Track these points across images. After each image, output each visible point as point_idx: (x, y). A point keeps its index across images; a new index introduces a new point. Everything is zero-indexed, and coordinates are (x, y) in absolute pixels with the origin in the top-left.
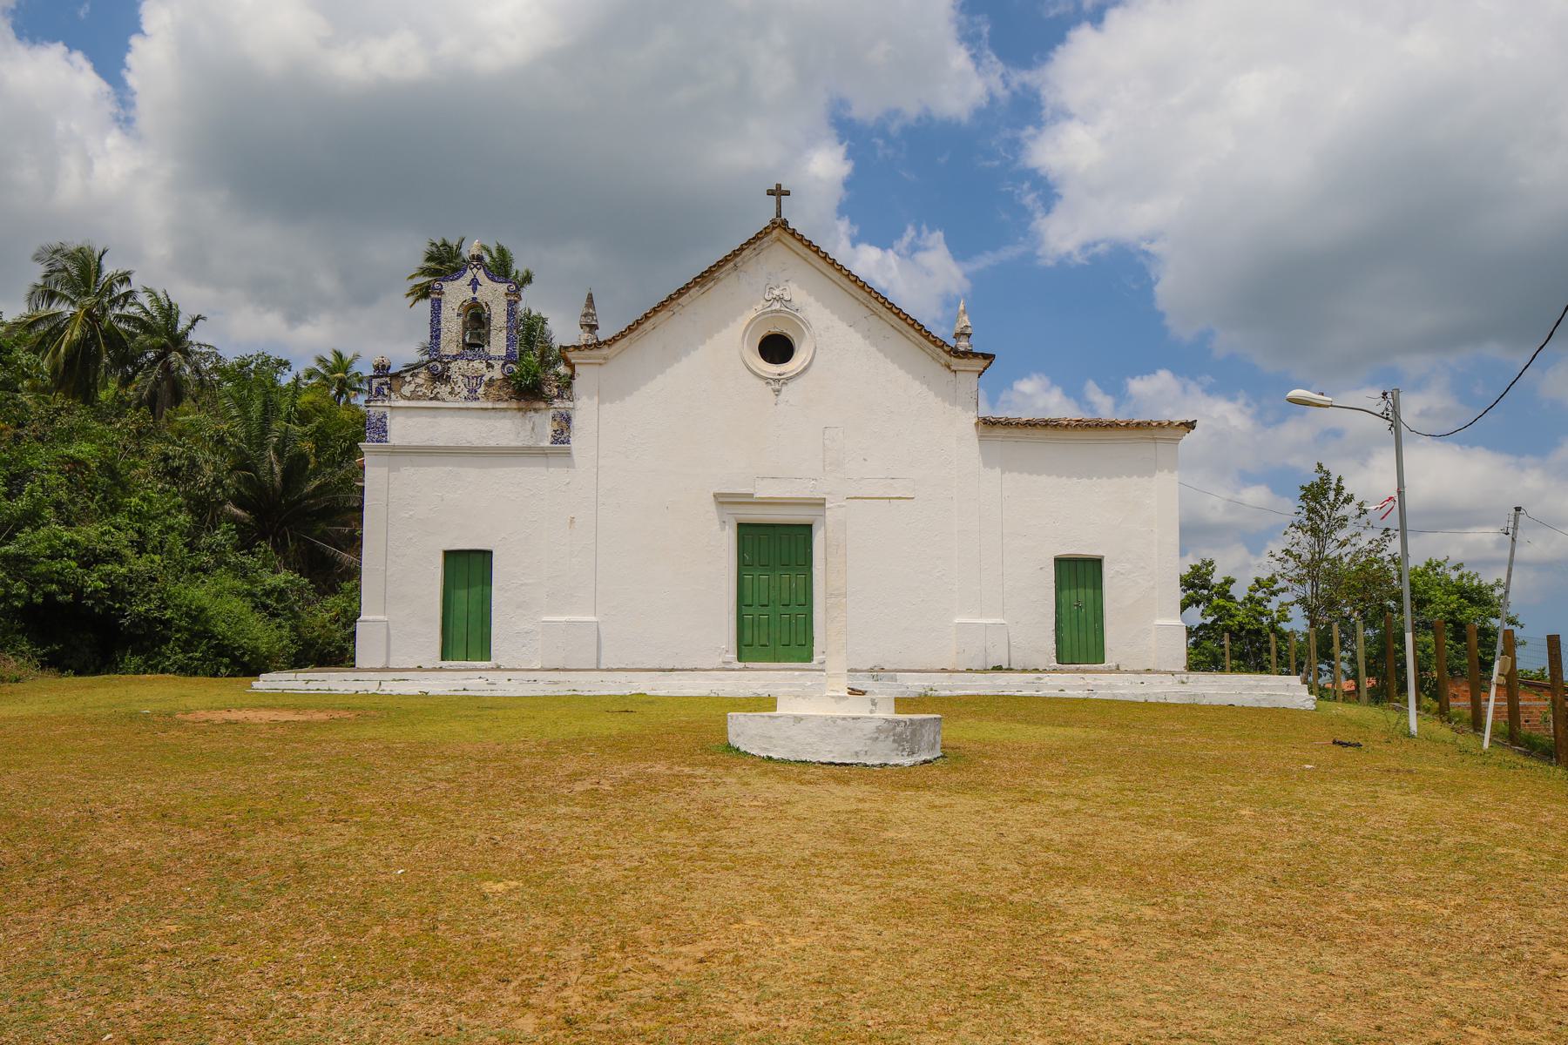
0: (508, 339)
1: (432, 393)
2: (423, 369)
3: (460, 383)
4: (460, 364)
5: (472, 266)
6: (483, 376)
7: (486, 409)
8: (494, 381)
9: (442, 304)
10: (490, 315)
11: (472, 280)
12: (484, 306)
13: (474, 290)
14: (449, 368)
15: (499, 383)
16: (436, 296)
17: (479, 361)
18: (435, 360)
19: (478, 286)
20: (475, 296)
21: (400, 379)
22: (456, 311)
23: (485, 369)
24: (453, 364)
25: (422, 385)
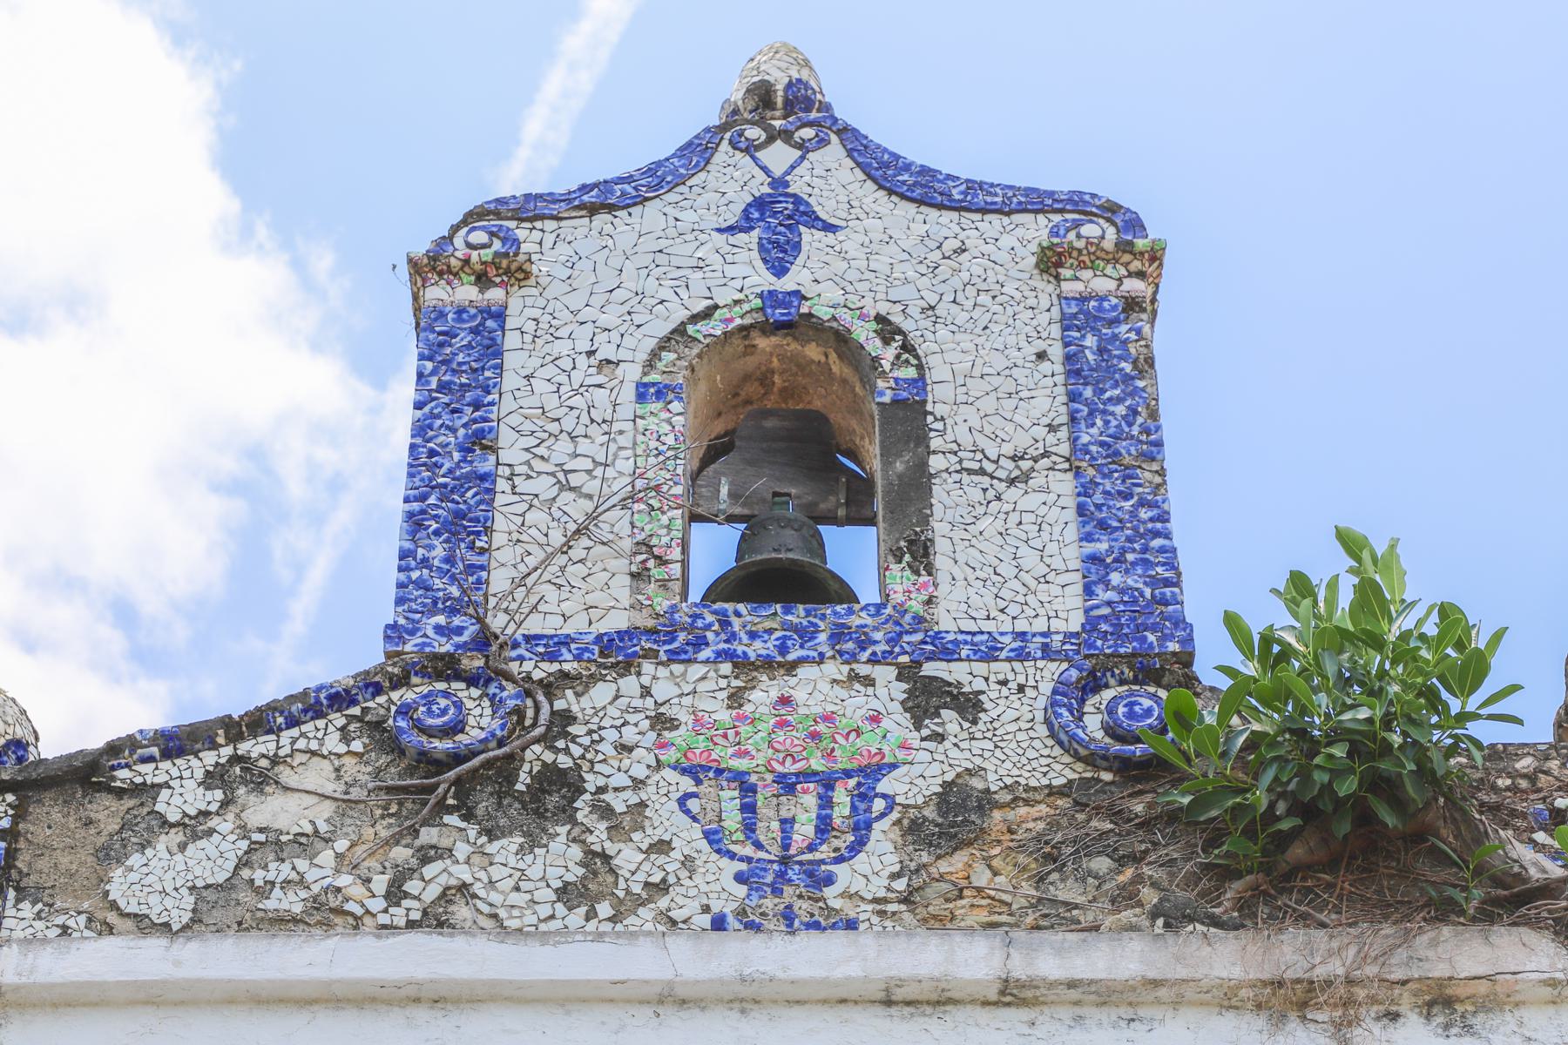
0: (1091, 519)
1: (395, 894)
2: (327, 734)
3: (665, 819)
4: (663, 690)
5: (754, 133)
6: (875, 770)
7: (941, 1000)
8: (986, 802)
9: (511, 340)
10: (920, 382)
11: (760, 203)
12: (874, 346)
13: (779, 256)
14: (567, 718)
15: (1032, 817)
16: (467, 292)
17: (835, 669)
18: (445, 668)
19: (810, 238)
20: (787, 284)
21: (107, 812)
22: (631, 373)
23: (897, 724)
24: (601, 693)
25: (306, 843)
